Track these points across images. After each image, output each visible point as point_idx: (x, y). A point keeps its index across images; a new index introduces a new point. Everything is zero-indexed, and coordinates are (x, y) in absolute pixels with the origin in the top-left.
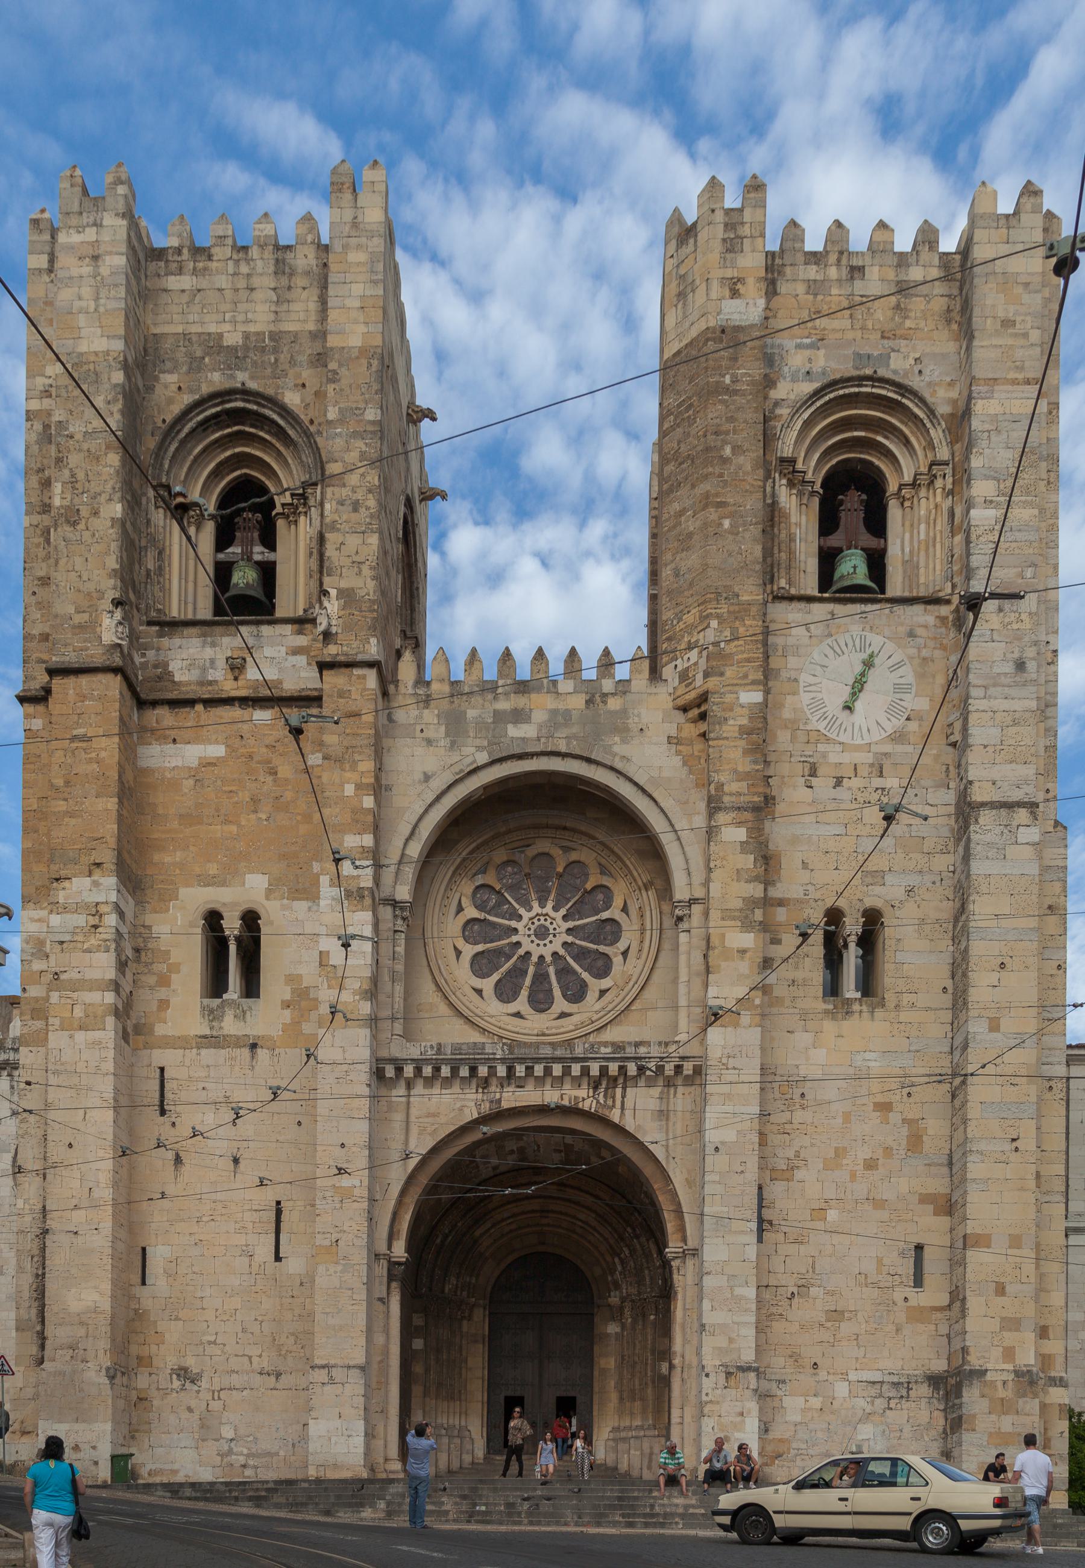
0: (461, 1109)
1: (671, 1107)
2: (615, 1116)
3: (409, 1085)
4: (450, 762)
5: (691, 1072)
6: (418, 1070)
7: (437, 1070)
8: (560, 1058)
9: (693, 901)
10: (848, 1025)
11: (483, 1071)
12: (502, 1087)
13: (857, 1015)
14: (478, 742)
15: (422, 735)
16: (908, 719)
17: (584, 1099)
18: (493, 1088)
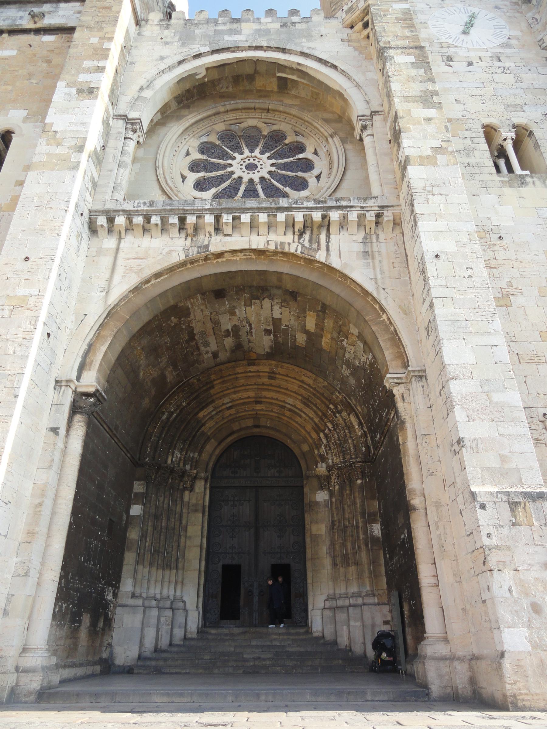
0: (169, 253)
1: (375, 249)
2: (321, 256)
3: (120, 239)
4: (180, 51)
5: (392, 218)
6: (130, 219)
7: (148, 219)
8: (266, 208)
9: (374, 113)
10: (524, 191)
11: (191, 219)
12: (211, 235)
13: (531, 185)
14: (202, 43)
15: (162, 40)
16: (509, 38)
17: (289, 244)
18: (201, 237)
